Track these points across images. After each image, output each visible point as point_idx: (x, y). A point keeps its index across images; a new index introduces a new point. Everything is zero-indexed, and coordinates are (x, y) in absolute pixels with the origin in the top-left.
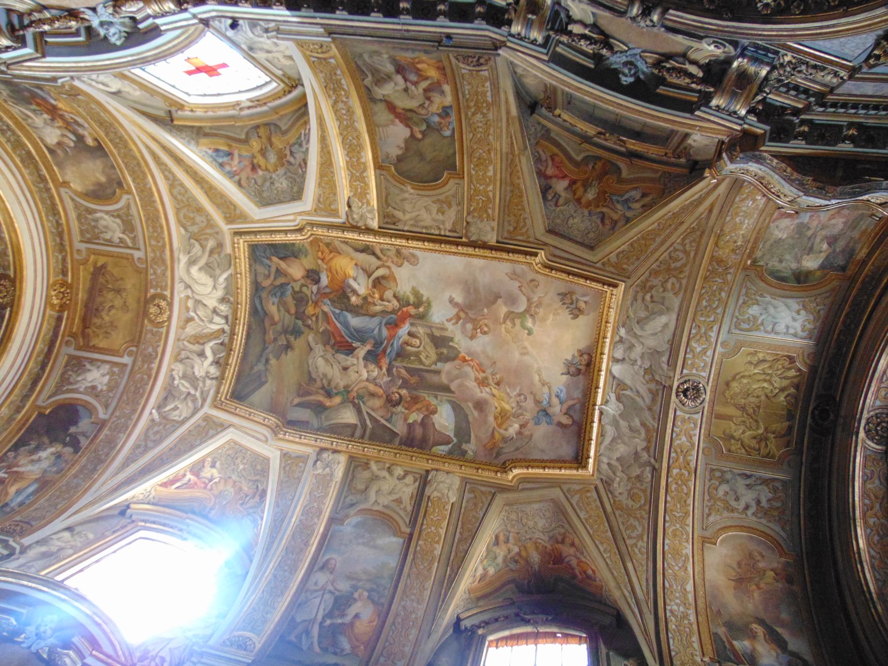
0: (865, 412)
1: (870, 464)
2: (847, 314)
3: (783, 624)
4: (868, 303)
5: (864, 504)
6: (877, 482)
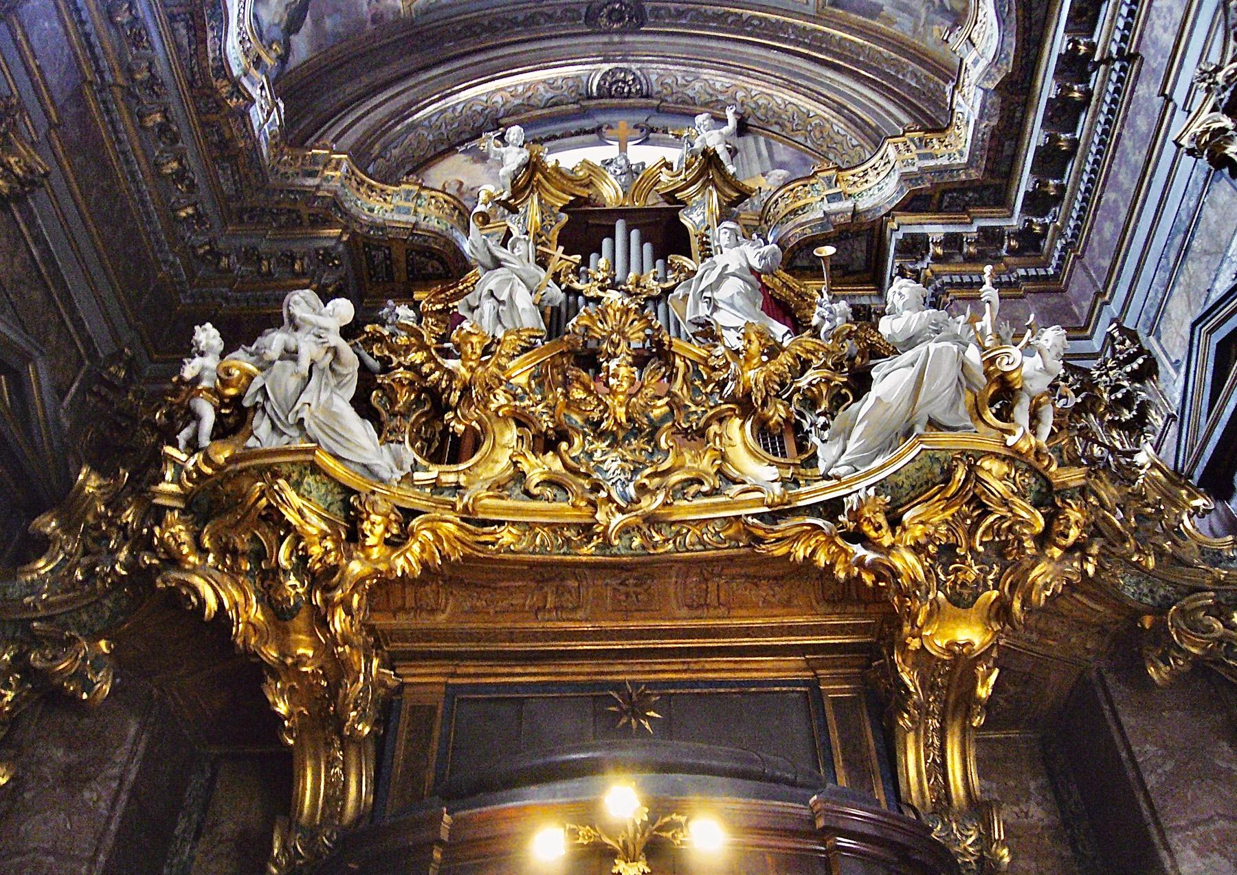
0: (639, 65)
1: (570, 83)
2: (766, 18)
3: (317, 23)
4: (785, 41)
5: (516, 86)
6: (549, 95)
